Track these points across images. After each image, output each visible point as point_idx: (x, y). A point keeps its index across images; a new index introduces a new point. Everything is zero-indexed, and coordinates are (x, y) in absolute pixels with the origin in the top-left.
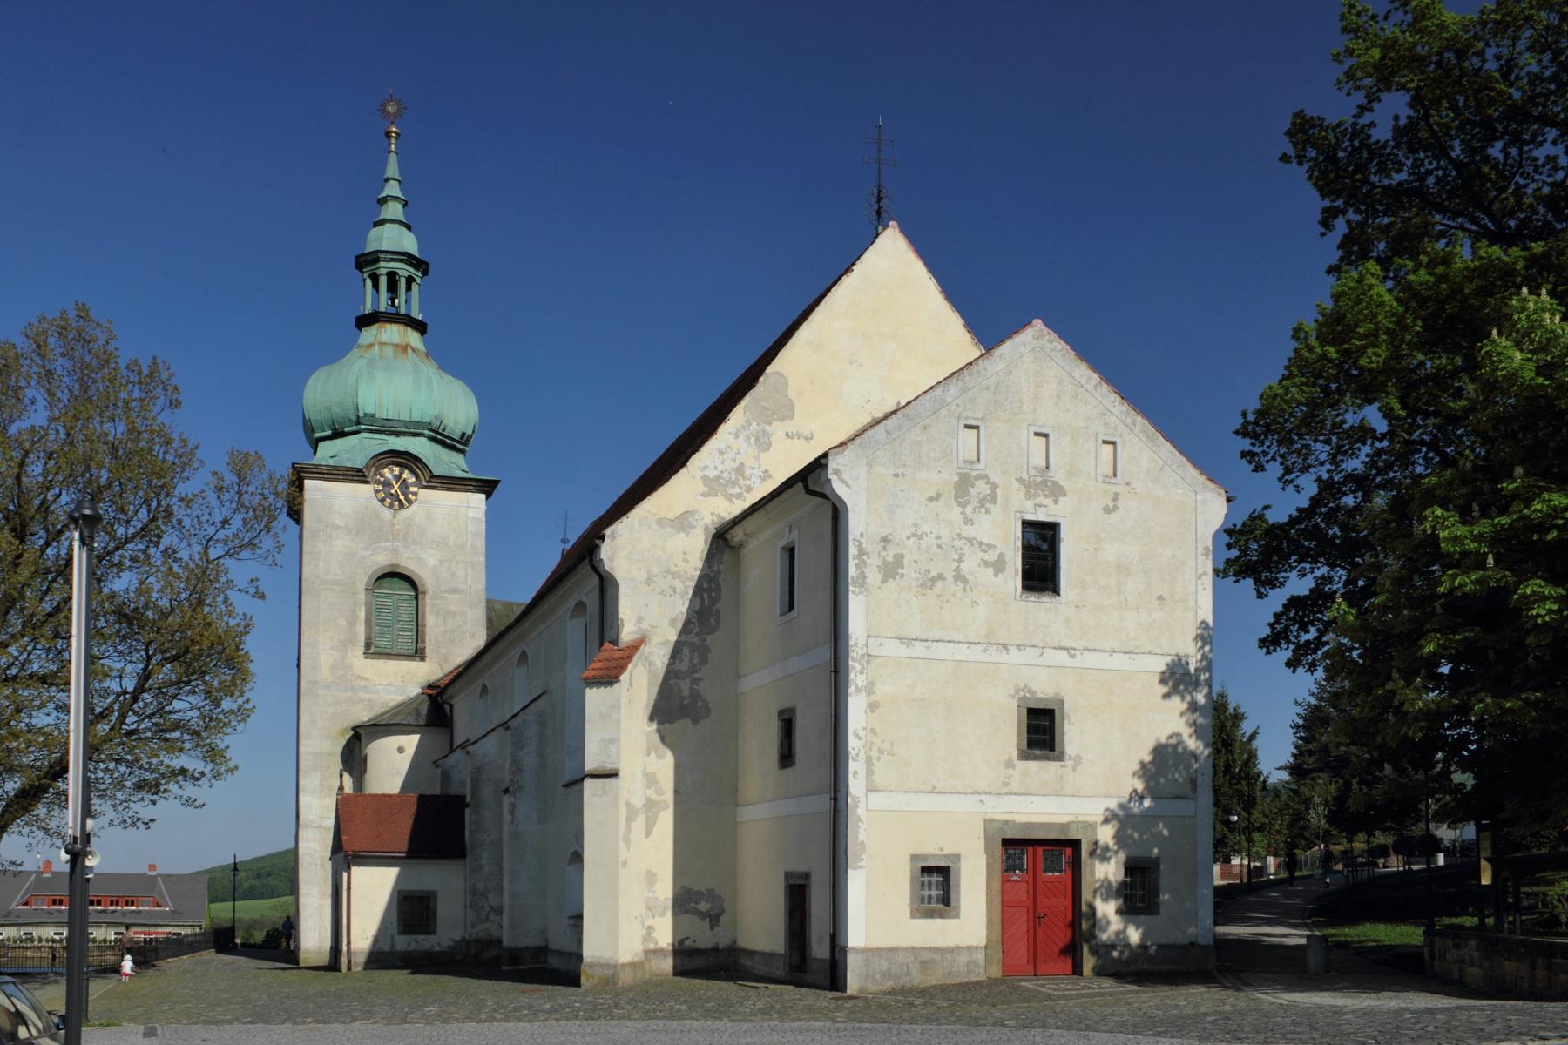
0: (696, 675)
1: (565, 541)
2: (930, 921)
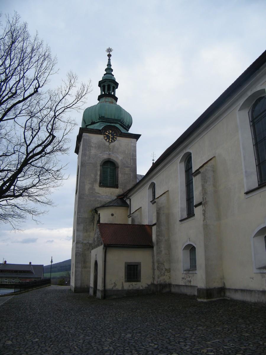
1: (153, 160)
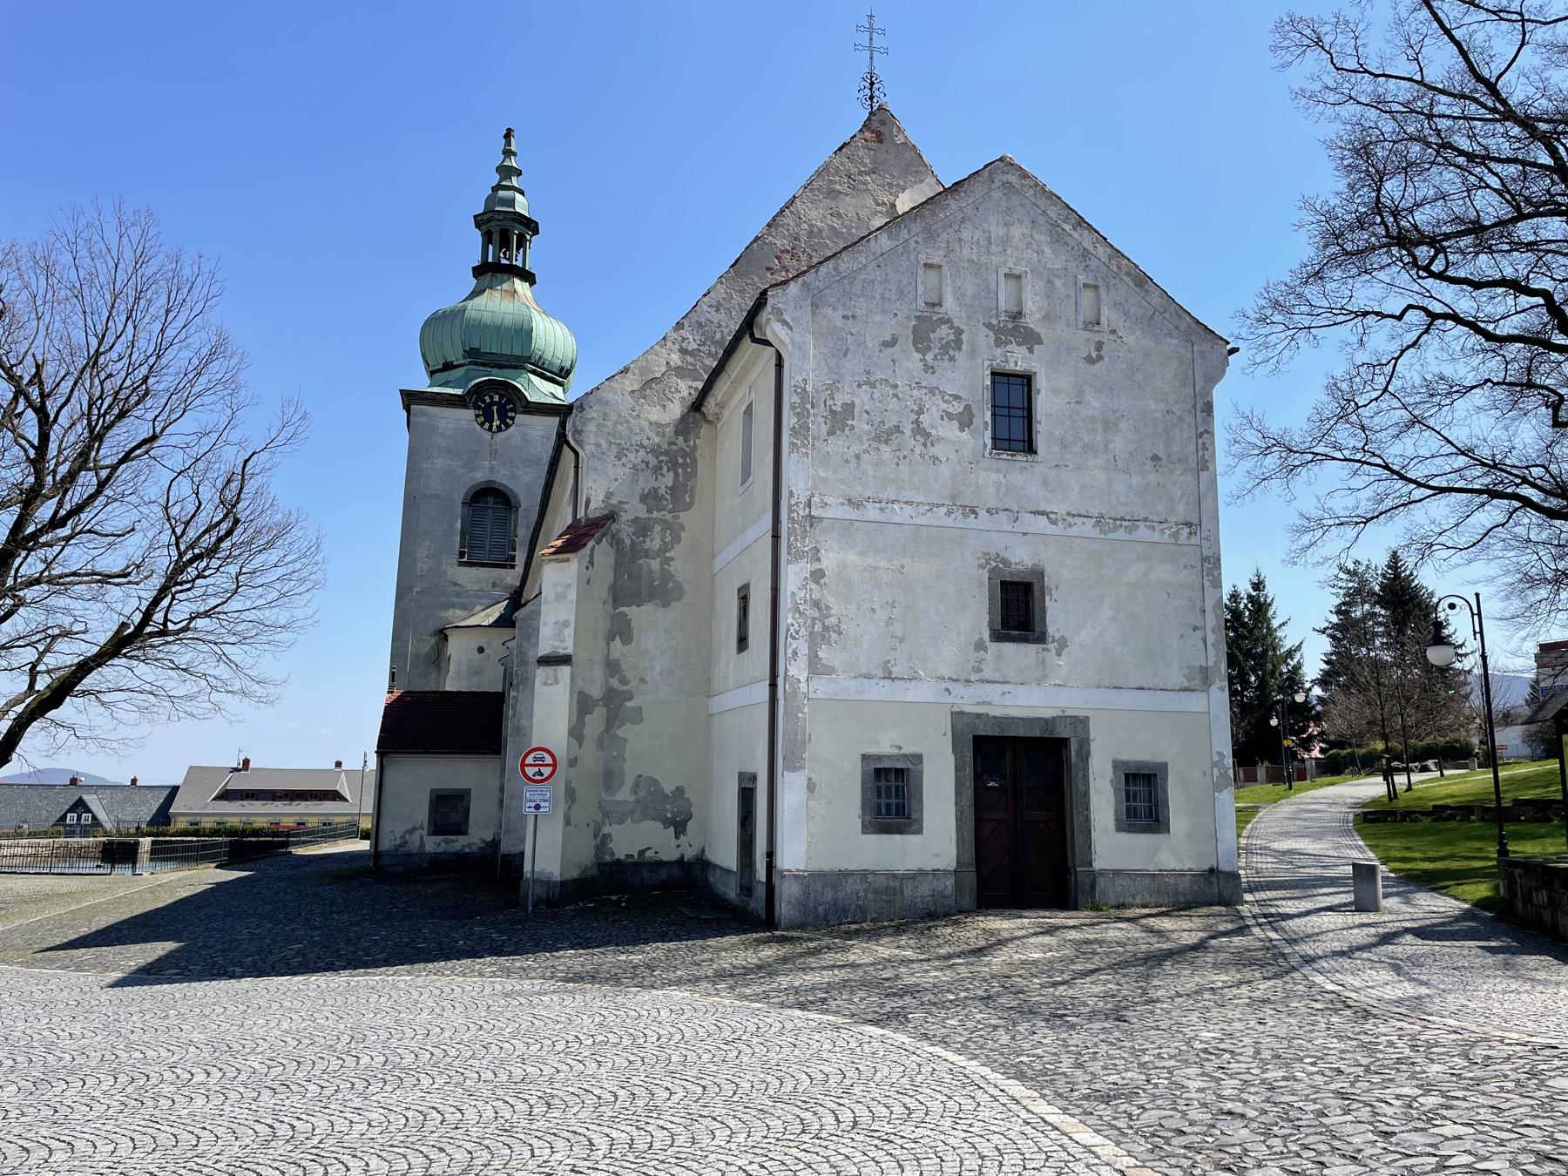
0: (667, 555)
2: (885, 836)
